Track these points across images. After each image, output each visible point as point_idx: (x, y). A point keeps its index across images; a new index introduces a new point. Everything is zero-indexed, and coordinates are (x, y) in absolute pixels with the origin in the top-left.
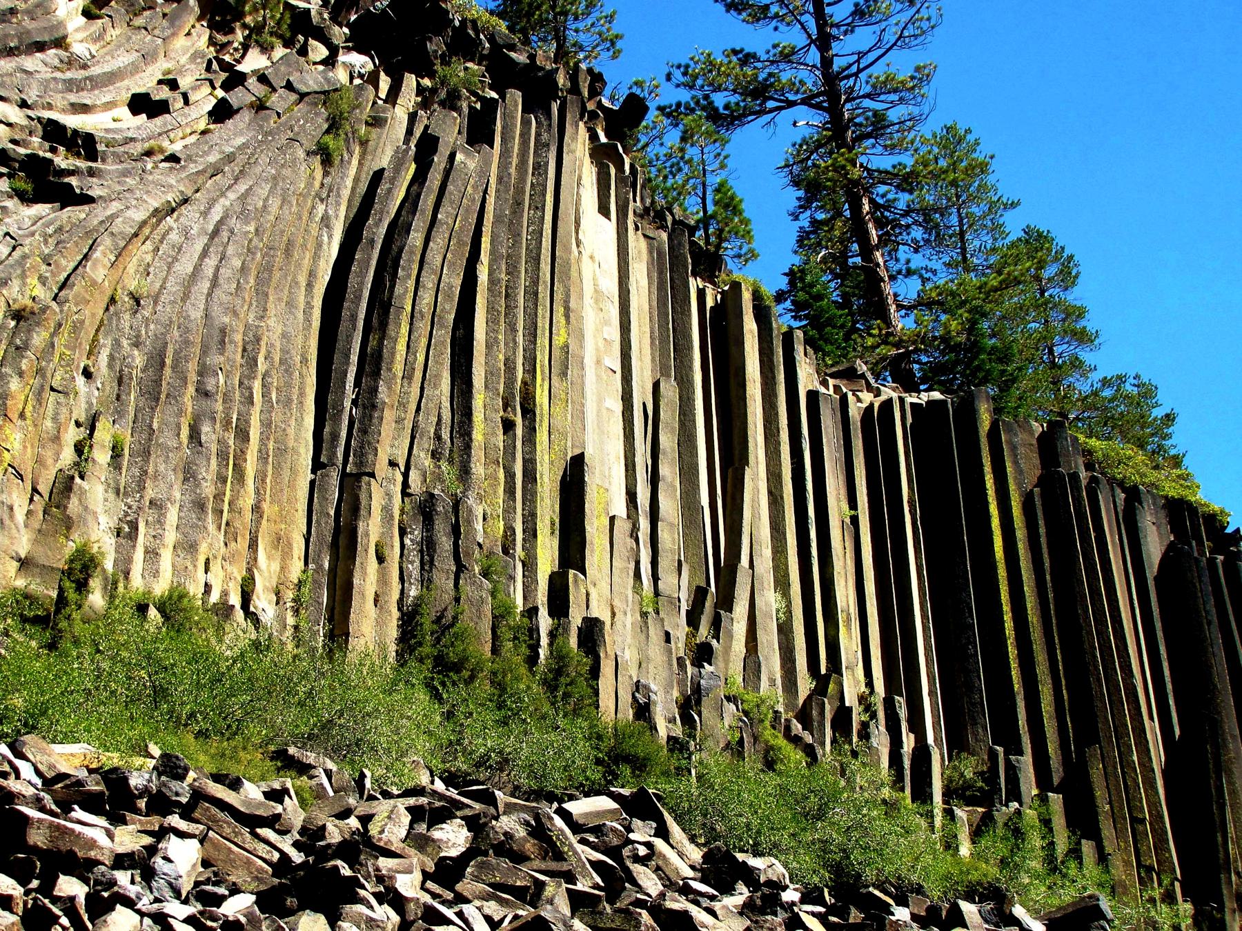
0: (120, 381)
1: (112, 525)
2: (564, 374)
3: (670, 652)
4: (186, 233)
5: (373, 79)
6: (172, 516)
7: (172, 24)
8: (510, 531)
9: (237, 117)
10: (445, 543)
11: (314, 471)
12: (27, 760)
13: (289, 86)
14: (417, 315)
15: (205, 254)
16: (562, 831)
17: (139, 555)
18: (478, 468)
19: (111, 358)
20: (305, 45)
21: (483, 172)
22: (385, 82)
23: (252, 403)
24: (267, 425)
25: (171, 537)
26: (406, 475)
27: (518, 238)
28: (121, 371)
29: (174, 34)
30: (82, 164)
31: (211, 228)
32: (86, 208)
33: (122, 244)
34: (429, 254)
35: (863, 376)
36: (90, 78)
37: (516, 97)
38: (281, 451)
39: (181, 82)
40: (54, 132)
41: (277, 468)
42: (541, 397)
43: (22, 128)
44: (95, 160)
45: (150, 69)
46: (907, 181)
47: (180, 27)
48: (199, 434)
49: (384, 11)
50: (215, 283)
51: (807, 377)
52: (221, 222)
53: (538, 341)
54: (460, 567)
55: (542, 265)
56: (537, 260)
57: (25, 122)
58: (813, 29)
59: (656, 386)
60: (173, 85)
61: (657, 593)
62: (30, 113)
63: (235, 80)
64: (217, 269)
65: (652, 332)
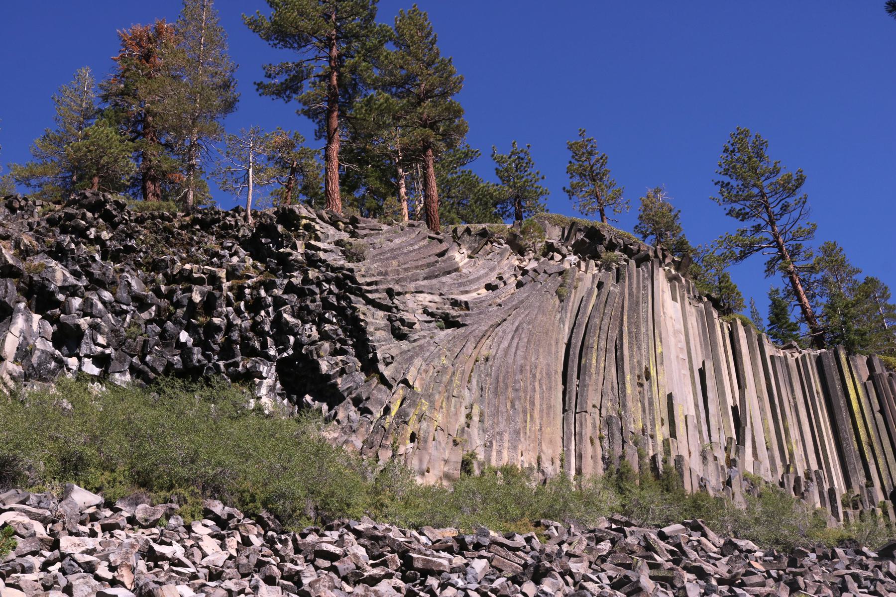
0: (482, 390)
2: (662, 363)
3: (717, 465)
4: (504, 332)
5: (579, 265)
6: (506, 437)
7: (501, 256)
8: (645, 425)
9: (525, 286)
10: (617, 434)
11: (563, 413)
12: (425, 535)
13: (545, 272)
15: (513, 338)
16: (654, 539)
17: (494, 453)
18: (630, 404)
19: (478, 381)
20: (553, 256)
21: (622, 293)
22: (583, 264)
23: (535, 391)
24: (542, 398)
25: (506, 444)
26: (600, 410)
30: (462, 313)
31: (514, 328)
32: (464, 328)
33: (478, 339)
34: (602, 326)
35: (795, 347)
36: (469, 281)
37: (633, 262)
38: (549, 407)
39: (504, 277)
40: (455, 303)
41: (548, 414)
42: (653, 373)
43: (441, 303)
44: (469, 310)
45: (493, 274)
46: (812, 269)
48: (514, 405)
49: (582, 239)
50: (517, 348)
51: (769, 350)
54: (624, 442)
56: (647, 322)
57: (442, 301)
58: (767, 219)
59: (703, 363)
60: (501, 278)
61: (711, 443)
62: (443, 297)
63: (525, 272)
64: (518, 343)
65: (701, 342)
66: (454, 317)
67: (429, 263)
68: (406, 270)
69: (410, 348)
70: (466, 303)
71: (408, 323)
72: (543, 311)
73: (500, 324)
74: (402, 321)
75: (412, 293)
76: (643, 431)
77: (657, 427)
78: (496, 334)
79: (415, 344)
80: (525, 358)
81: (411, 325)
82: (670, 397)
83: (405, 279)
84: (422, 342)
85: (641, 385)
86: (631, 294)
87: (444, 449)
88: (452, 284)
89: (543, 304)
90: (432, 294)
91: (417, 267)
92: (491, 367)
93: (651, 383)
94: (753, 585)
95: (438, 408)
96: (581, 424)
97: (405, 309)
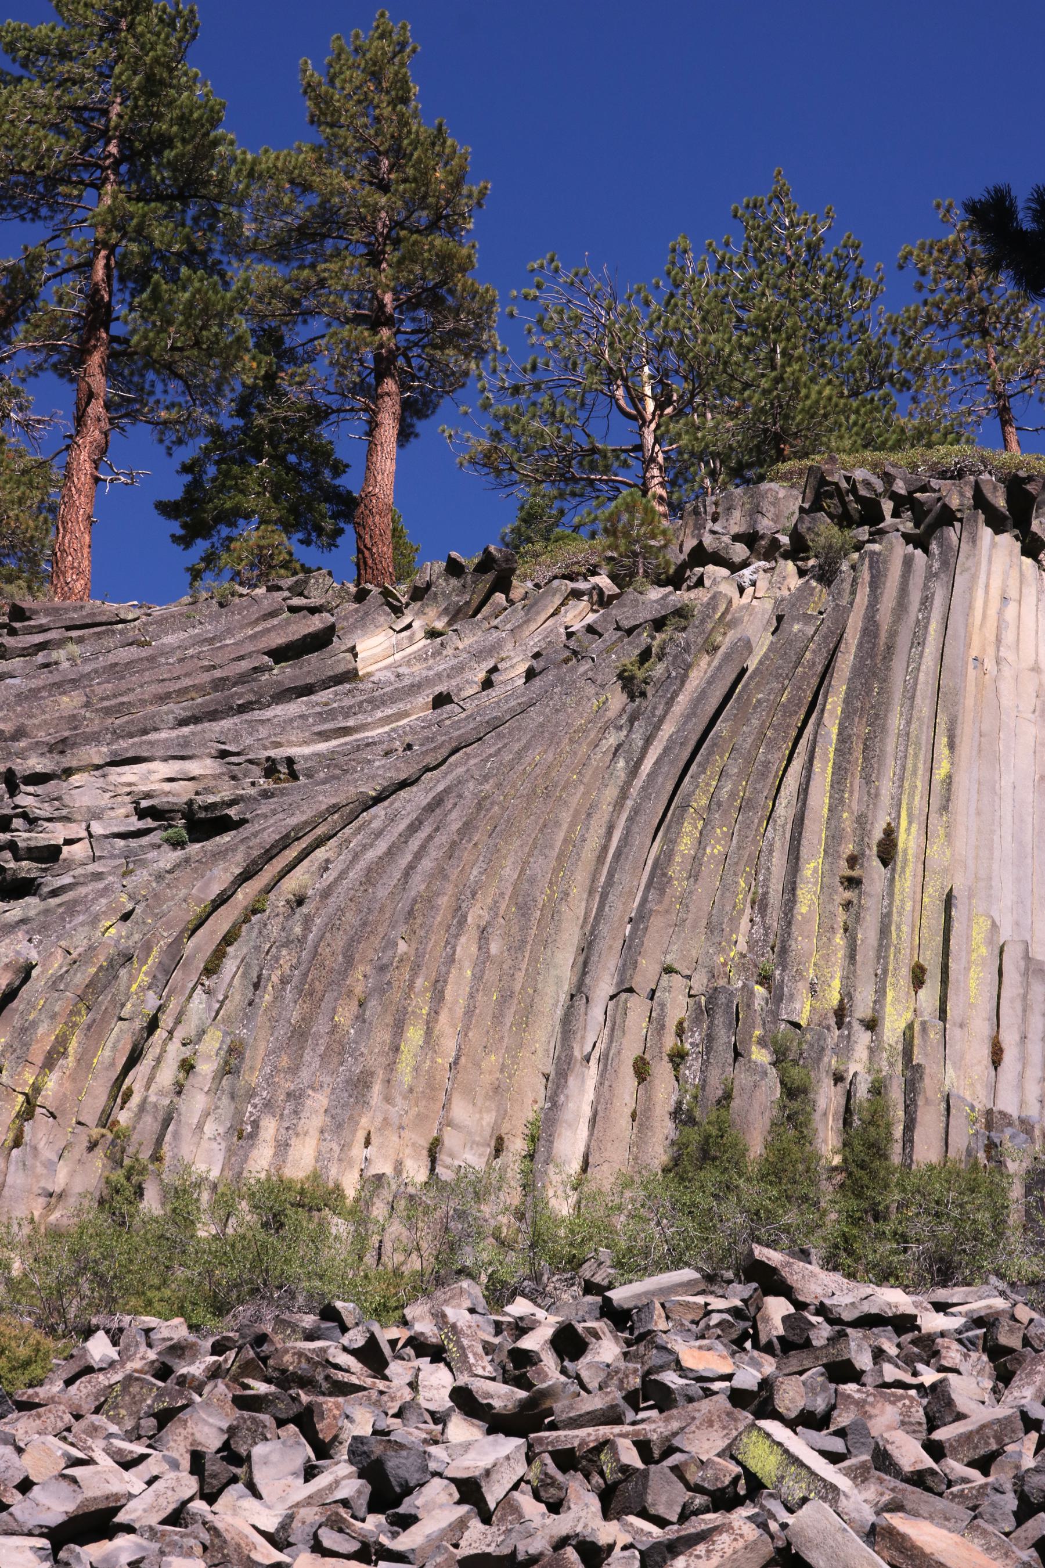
0: (256, 986)
1: (221, 1130)
2: (945, 808)
6: (318, 1101)
8: (847, 995)
13: (618, 628)
14: (714, 807)
15: (414, 828)
23: (453, 961)
27: (884, 685)
28: (259, 977)
29: (527, 622)
31: (424, 803)
42: (907, 841)
43: (216, 777)
47: (538, 613)
50: (418, 856)
52: (447, 791)
53: (906, 784)
55: (918, 700)
64: (430, 838)
66: (213, 806)
67: (223, 679)
68: (108, 711)
69: (32, 913)
70: (290, 761)
71: (29, 849)
72: (553, 735)
73: (377, 800)
74: (12, 846)
75: (98, 767)
76: (840, 1014)
77: (890, 995)
78: (358, 830)
79: (53, 902)
80: (440, 873)
81: (50, 854)
82: (949, 901)
83: (94, 738)
84: (82, 890)
85: (852, 883)
86: (870, 630)
87: (51, 1167)
88: (291, 720)
89: (561, 716)
90: (183, 758)
91: (163, 698)
92: (308, 921)
93: (894, 870)
94: (576, 1423)
95: (39, 1059)
96: (613, 1030)
97: (57, 814)
